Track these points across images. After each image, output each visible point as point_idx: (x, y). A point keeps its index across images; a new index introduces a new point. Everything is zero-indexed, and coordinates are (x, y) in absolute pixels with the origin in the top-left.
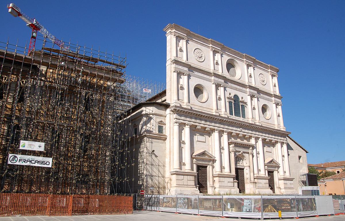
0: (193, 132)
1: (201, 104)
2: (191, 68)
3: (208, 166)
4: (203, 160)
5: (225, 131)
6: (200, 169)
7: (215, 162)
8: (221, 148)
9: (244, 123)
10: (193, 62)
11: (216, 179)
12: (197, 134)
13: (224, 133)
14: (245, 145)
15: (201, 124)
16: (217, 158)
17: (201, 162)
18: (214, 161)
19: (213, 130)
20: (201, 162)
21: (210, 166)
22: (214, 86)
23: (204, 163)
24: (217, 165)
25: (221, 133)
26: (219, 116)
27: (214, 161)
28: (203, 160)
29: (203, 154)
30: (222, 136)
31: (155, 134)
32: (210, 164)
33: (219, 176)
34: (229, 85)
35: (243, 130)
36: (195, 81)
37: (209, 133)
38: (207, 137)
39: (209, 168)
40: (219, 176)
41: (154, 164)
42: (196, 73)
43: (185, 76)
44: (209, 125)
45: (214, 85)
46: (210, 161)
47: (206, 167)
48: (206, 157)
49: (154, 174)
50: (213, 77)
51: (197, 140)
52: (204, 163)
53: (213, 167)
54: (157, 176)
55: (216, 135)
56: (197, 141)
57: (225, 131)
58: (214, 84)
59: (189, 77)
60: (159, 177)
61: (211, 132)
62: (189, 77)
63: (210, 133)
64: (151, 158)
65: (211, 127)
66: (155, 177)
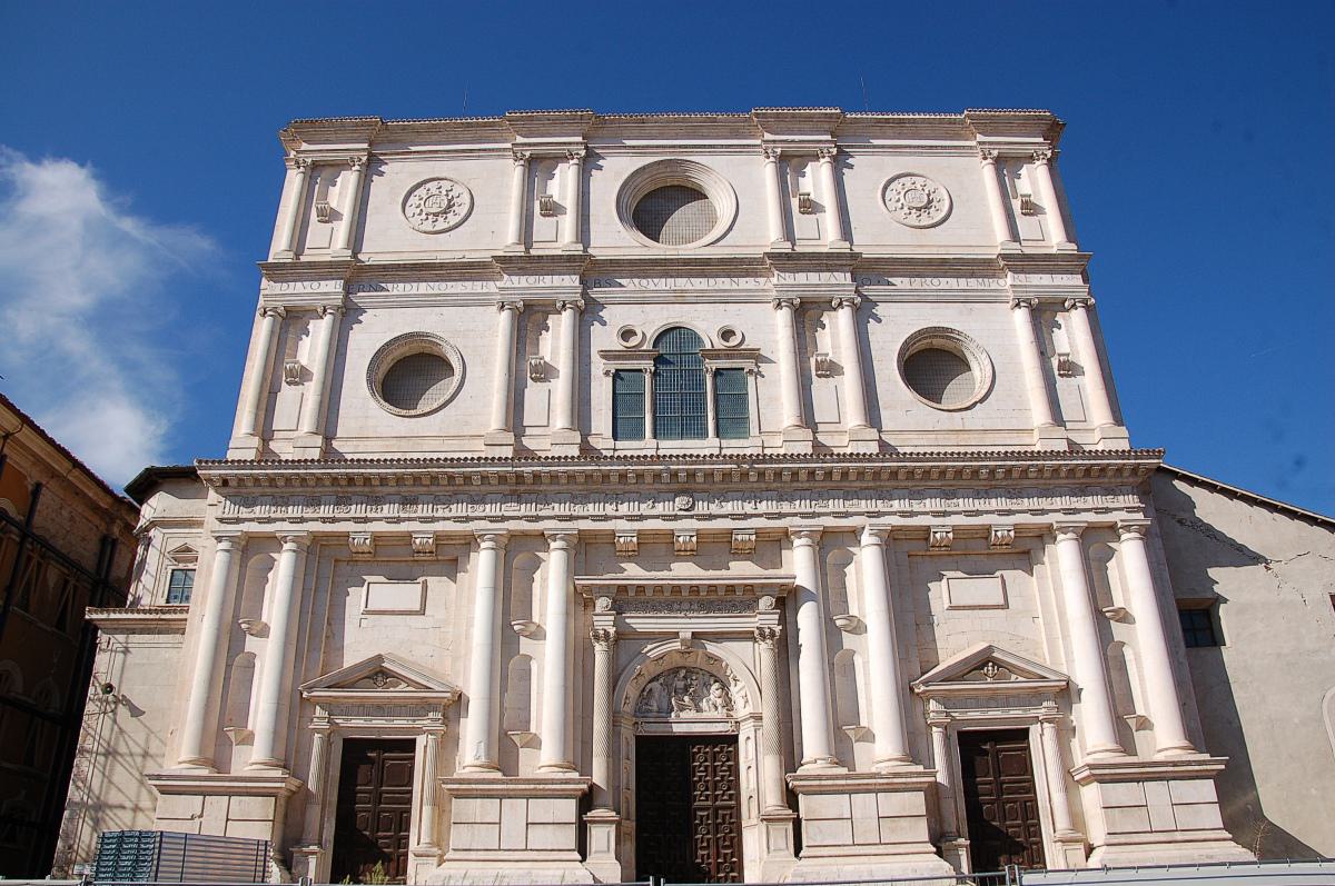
0: (349, 568)
1: (957, 420)
2: (868, 271)
3: (1034, 730)
4: (379, 707)
5: (1120, 524)
6: (986, 753)
7: (1075, 698)
8: (1104, 617)
9: (693, 463)
10: (879, 234)
11: (1091, 795)
12: (368, 579)
13: (1055, 538)
14: (649, 593)
15: (939, 516)
16: (1084, 670)
17: (974, 714)
18: (1067, 694)
19: (1046, 535)
20: (974, 714)
21: (1046, 725)
22: (1021, 317)
23: (379, 722)
24: (1091, 717)
25: (1095, 544)
26: (1074, 449)
27: (1067, 694)
28: (380, 709)
29: (983, 662)
30: (1113, 551)
31: (150, 612)
32: (1041, 712)
33: (1104, 775)
34: (631, 287)
35: (701, 508)
36: (896, 326)
37: (1025, 550)
38: (1014, 576)
39: (1042, 744)
40: (1104, 775)
41: (122, 749)
42: (630, 284)
43: (840, 311)
44: (1000, 516)
45: (506, 314)
46: (1036, 697)
47: (1023, 734)
48: (1016, 682)
49: (114, 797)
50: (1010, 274)
51: (946, 606)
52: (379, 722)
53: (1065, 732)
54: (128, 804)
55: (1064, 555)
56: (952, 608)
57: (1120, 524)
58: (1018, 305)
59: (863, 313)
60: (136, 809)
61: (1028, 544)
62: (863, 313)
63: (1027, 552)
64: (110, 722)
65: (439, 526)
66: (120, 813)
